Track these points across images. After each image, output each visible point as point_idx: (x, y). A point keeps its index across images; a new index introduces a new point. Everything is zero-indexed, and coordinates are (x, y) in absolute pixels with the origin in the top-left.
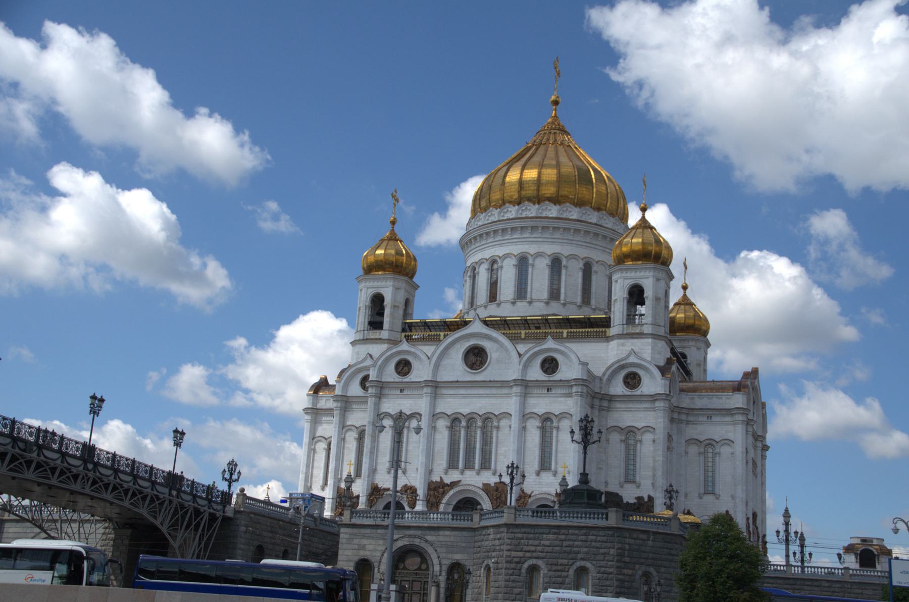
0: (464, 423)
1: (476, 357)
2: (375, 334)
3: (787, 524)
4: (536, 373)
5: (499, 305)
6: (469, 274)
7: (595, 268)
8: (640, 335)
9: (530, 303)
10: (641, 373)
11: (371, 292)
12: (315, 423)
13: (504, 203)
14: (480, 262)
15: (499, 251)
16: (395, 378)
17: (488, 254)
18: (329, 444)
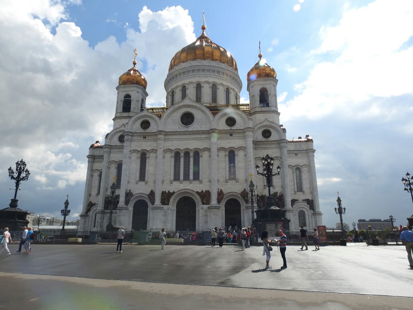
0: (182, 154)
1: (187, 119)
2: (125, 114)
3: (339, 204)
4: (222, 125)
6: (170, 94)
7: (231, 91)
8: (269, 112)
10: (271, 130)
11: (123, 94)
12: (93, 163)
13: (187, 61)
15: (186, 81)
16: (141, 130)
17: (180, 83)
18: (101, 173)
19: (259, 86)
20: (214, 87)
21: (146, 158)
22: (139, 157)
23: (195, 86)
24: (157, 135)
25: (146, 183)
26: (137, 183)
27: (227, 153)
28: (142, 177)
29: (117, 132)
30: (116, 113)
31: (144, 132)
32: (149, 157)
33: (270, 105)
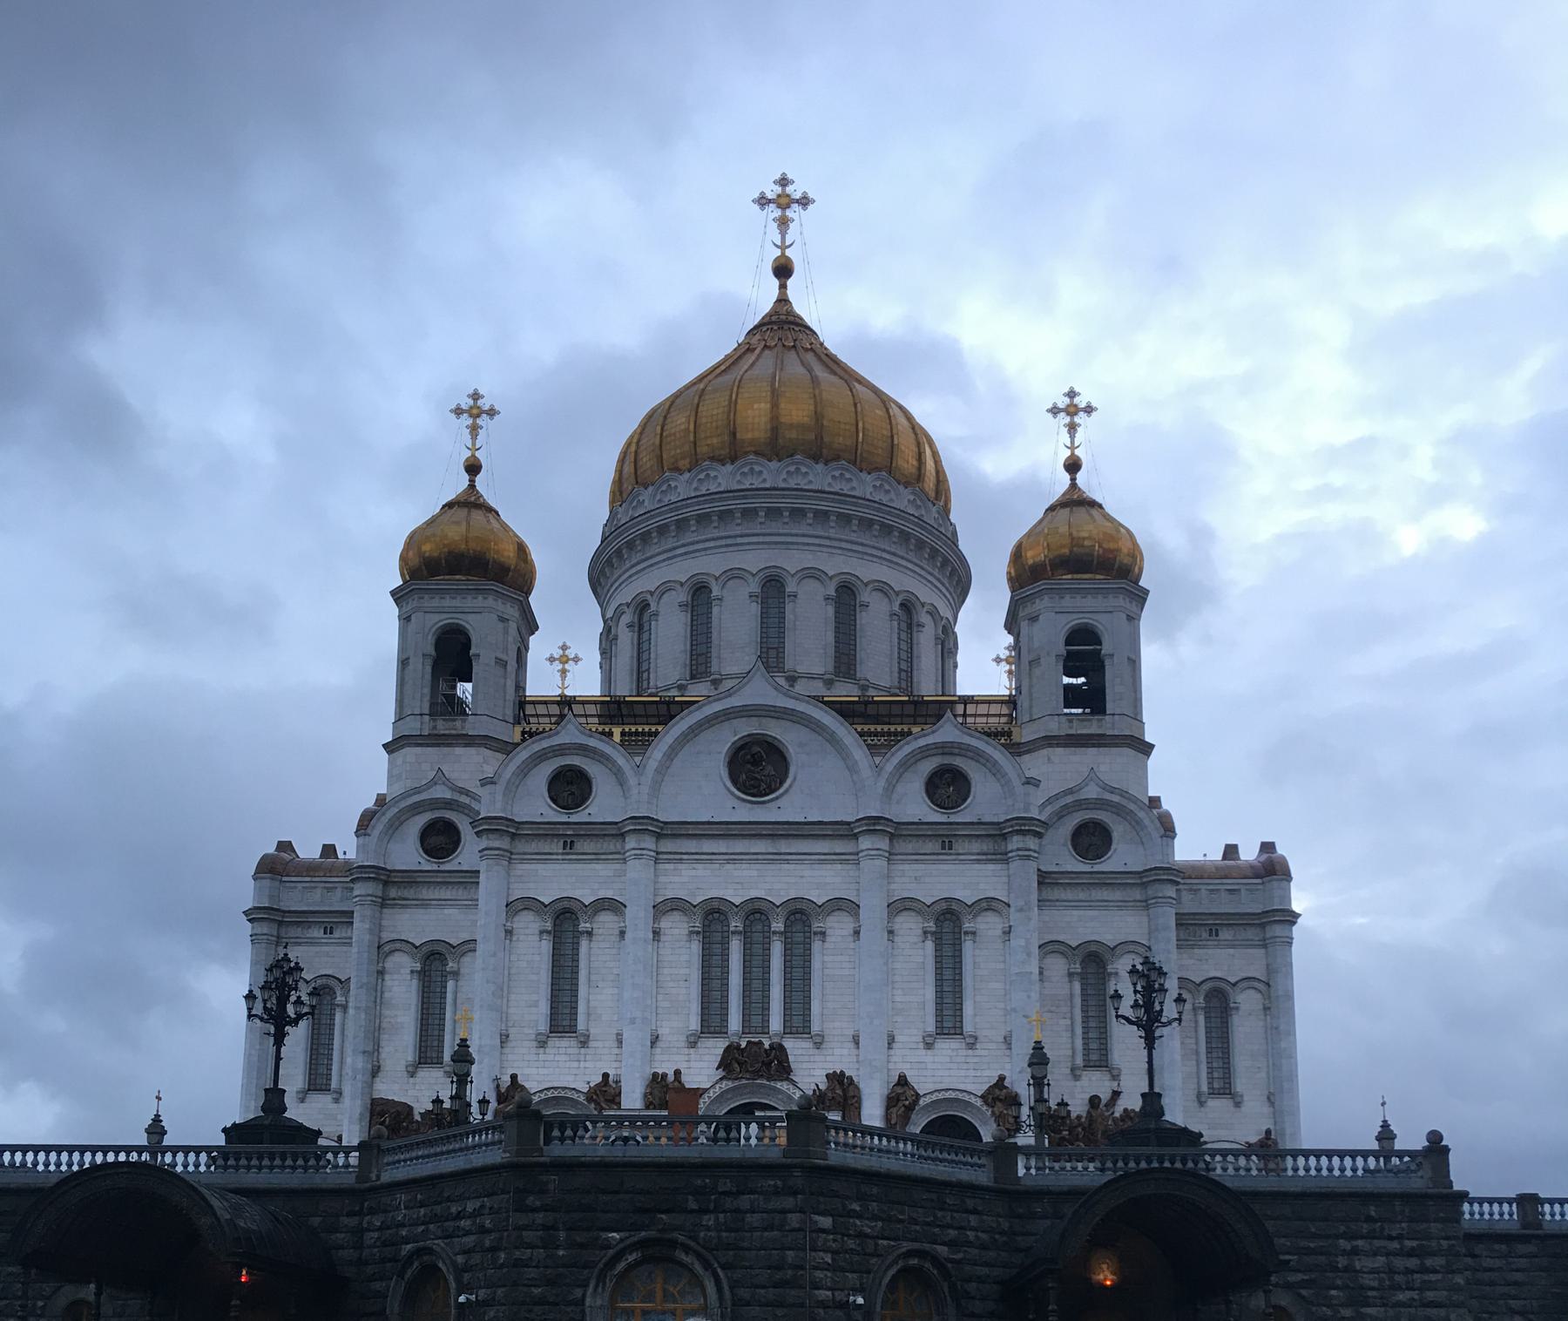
0: (736, 924)
1: (757, 767)
5: (716, 683)
6: (626, 619)
9: (792, 680)
14: (665, 588)
15: (710, 564)
16: (552, 814)
17: (682, 570)
19: (1063, 619)
20: (846, 597)
21: (577, 935)
22: (549, 932)
23: (754, 586)
24: (623, 835)
25: (584, 1042)
26: (542, 1044)
27: (931, 926)
28: (563, 1019)
29: (416, 809)
30: (400, 718)
31: (564, 819)
32: (590, 934)
33: (1110, 708)
